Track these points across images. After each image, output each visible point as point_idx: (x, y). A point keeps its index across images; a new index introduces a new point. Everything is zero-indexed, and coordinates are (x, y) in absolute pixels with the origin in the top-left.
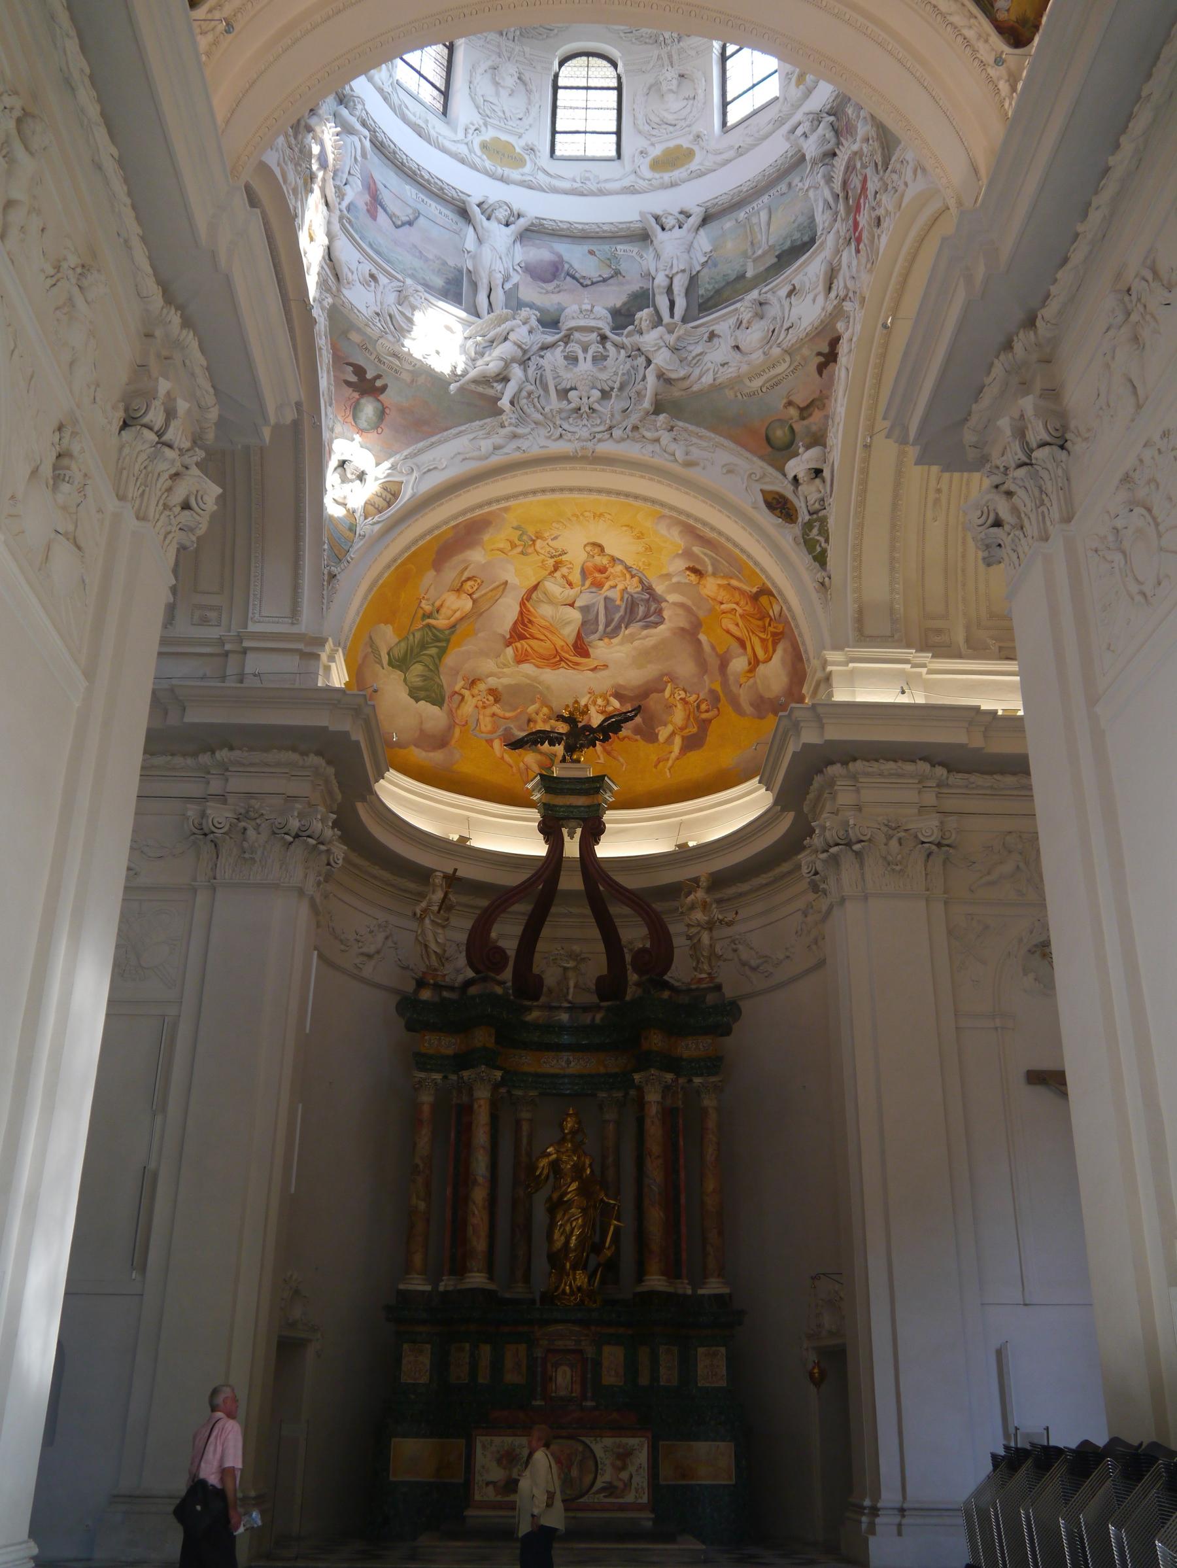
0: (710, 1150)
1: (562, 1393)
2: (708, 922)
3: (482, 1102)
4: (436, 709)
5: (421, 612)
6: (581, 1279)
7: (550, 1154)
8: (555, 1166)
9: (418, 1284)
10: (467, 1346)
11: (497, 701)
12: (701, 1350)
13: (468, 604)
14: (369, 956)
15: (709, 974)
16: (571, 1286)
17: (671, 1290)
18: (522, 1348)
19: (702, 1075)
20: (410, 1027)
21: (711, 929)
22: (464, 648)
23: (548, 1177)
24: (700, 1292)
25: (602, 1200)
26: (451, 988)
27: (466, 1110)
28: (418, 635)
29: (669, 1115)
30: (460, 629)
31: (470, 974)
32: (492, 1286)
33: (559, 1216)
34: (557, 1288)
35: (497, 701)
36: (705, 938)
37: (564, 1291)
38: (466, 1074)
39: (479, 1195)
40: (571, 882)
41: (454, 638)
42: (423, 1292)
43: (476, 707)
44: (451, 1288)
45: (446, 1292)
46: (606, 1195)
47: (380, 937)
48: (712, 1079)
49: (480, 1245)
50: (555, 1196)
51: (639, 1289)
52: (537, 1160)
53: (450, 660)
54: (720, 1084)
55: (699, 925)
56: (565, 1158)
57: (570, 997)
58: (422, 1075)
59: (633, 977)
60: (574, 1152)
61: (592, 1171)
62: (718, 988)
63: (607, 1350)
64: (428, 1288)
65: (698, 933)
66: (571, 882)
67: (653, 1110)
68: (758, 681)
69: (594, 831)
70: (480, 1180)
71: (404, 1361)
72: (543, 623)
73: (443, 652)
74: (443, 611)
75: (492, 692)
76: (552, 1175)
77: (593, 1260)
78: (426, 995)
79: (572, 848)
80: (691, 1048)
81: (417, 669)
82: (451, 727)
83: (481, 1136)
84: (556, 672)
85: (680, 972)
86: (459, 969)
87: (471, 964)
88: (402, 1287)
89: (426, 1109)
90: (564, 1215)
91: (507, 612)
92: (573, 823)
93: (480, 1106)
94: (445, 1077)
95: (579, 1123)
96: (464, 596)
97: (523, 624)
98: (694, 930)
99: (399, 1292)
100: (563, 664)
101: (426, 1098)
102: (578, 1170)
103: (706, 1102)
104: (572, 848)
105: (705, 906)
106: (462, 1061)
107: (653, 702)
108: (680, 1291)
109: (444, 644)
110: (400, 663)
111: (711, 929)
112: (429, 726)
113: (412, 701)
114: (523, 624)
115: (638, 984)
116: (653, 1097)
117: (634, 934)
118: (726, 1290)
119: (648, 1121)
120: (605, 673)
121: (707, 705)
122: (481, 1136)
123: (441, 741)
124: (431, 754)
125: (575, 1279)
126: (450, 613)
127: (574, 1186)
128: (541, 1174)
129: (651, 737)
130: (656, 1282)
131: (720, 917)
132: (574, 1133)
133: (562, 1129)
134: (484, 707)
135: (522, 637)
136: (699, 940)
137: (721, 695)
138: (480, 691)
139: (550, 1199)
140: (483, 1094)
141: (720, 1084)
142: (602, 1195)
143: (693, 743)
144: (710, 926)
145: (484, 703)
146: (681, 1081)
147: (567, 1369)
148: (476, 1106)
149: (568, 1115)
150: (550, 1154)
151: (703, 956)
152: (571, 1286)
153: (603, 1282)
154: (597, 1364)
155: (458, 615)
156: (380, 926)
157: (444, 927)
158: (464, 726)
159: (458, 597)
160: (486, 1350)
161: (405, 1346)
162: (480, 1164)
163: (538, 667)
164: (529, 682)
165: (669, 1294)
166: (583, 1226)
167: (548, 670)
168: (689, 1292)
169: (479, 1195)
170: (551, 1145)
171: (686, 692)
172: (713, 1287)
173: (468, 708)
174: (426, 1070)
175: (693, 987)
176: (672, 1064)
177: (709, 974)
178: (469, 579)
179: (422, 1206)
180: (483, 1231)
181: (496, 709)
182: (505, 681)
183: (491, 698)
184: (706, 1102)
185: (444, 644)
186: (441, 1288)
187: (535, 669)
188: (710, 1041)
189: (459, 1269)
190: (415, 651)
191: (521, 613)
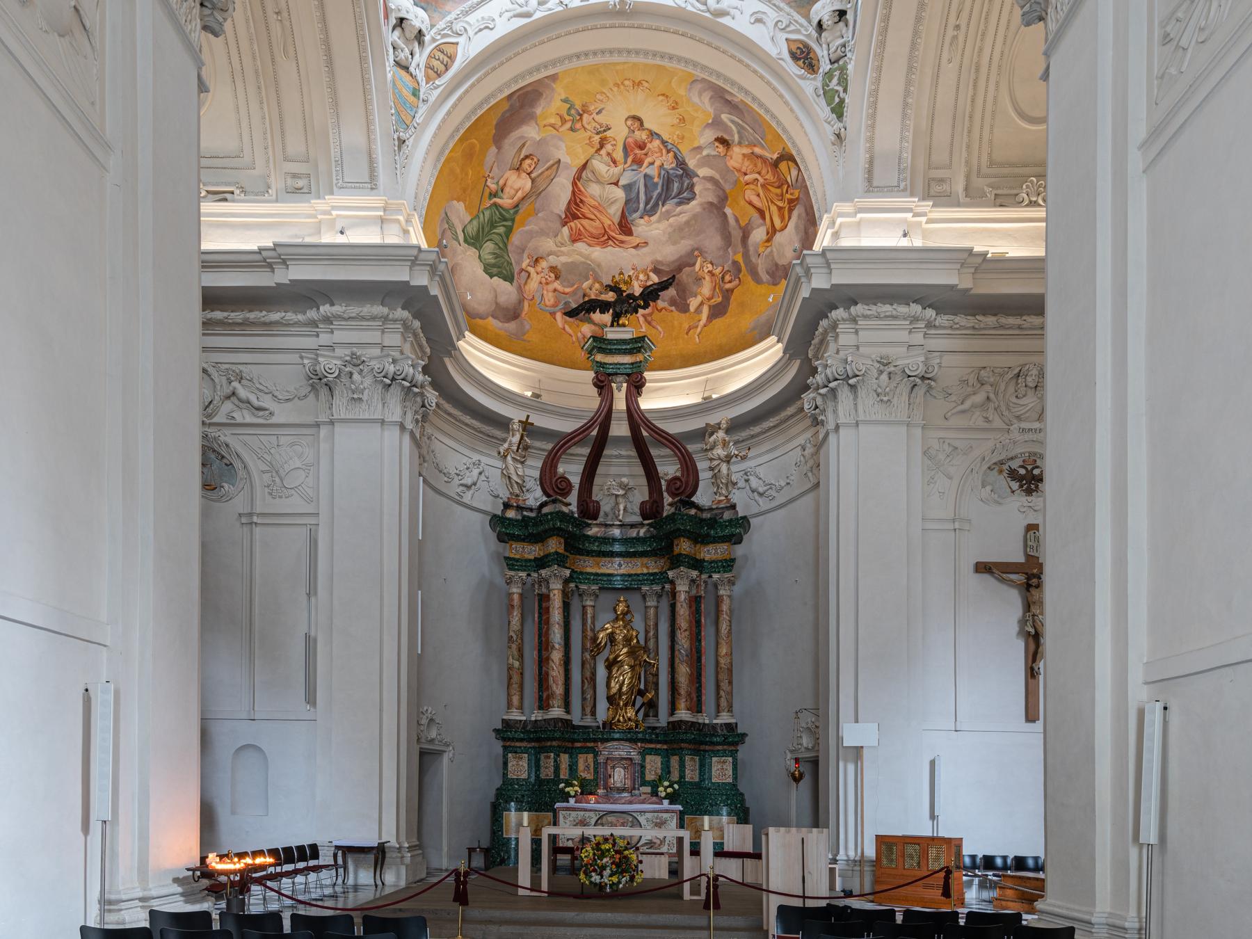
0: (724, 626)
1: (618, 785)
2: (726, 456)
3: (556, 592)
6: (630, 713)
7: (607, 629)
8: (611, 638)
9: (515, 715)
10: (552, 754)
11: (557, 278)
12: (714, 759)
14: (468, 487)
15: (726, 497)
16: (623, 716)
17: (694, 720)
18: (590, 756)
19: (719, 572)
20: (502, 538)
21: (728, 462)
23: (606, 644)
24: (715, 721)
25: (645, 661)
26: (531, 510)
27: (544, 599)
29: (695, 602)
31: (545, 499)
32: (568, 717)
33: (614, 671)
34: (613, 719)
35: (557, 278)
36: (724, 467)
37: (619, 721)
38: (543, 572)
39: (556, 656)
40: (619, 428)
42: (521, 721)
43: (541, 283)
44: (540, 718)
45: (536, 721)
46: (648, 657)
47: (476, 472)
48: (727, 575)
49: (558, 690)
50: (611, 657)
51: (671, 719)
52: (598, 632)
54: (732, 579)
55: (720, 459)
56: (618, 631)
57: (621, 517)
58: (512, 573)
59: (668, 499)
60: (625, 627)
61: (638, 641)
62: (733, 507)
63: (648, 758)
64: (524, 718)
65: (719, 465)
66: (619, 428)
67: (682, 597)
68: (774, 250)
69: (637, 386)
70: (557, 646)
71: (510, 765)
75: (553, 269)
76: (609, 644)
77: (639, 701)
78: (511, 514)
79: (620, 404)
80: (710, 553)
82: (521, 301)
83: (556, 616)
84: (606, 250)
85: (704, 497)
86: (534, 497)
87: (545, 493)
88: (505, 717)
89: (516, 597)
90: (618, 670)
92: (620, 378)
93: (554, 595)
94: (529, 575)
95: (628, 607)
98: (716, 463)
99: (503, 720)
100: (610, 242)
101: (516, 590)
102: (627, 640)
103: (721, 592)
104: (620, 404)
105: (725, 444)
106: (541, 563)
107: (684, 276)
108: (700, 721)
111: (728, 462)
115: (671, 505)
116: (682, 588)
117: (668, 468)
118: (733, 721)
119: (678, 605)
120: (645, 250)
121: (731, 276)
122: (556, 616)
123: (512, 314)
125: (626, 713)
127: (625, 650)
128: (600, 643)
129: (684, 308)
130: (683, 714)
131: (736, 452)
132: (625, 614)
133: (615, 611)
134: (547, 284)
136: (719, 471)
137: (743, 265)
138: (543, 269)
139: (607, 659)
140: (556, 587)
141: (732, 579)
142: (645, 657)
143: (718, 311)
144: (728, 459)
145: (546, 279)
146: (704, 576)
147: (622, 770)
148: (552, 595)
149: (620, 601)
150: (607, 629)
151: (722, 483)
152: (623, 716)
153: (646, 715)
154: (643, 767)
156: (474, 463)
157: (522, 463)
158: (532, 300)
160: (565, 759)
161: (510, 755)
162: (557, 635)
163: (590, 245)
164: (583, 260)
165: (693, 722)
166: (631, 678)
167: (598, 248)
168: (707, 722)
169: (556, 656)
170: (608, 623)
171: (712, 264)
172: (724, 718)
173: (533, 285)
174: (515, 570)
175: (714, 507)
176: (697, 564)
177: (726, 497)
179: (517, 664)
180: (561, 680)
181: (557, 285)
182: (563, 259)
183: (552, 275)
184: (721, 592)
186: (533, 719)
187: (587, 247)
188: (726, 547)
189: (543, 704)
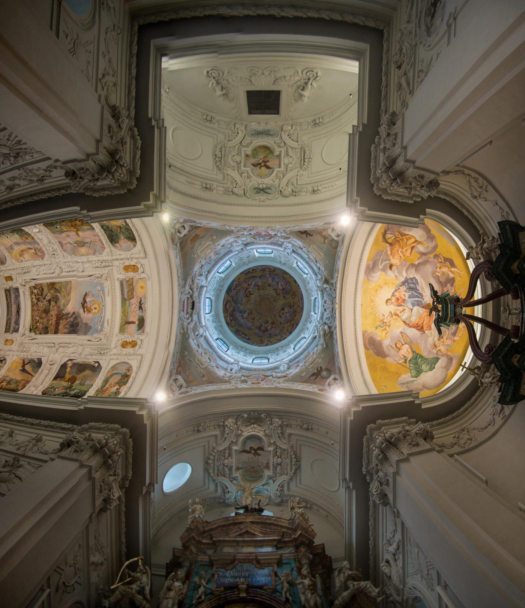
4: (440, 361)
5: (403, 364)
13: (407, 346)
22: (422, 349)
28: (411, 365)
30: (415, 349)
41: (418, 352)
53: (425, 354)
72: (418, 320)
73: (421, 357)
74: (405, 355)
81: (424, 367)
91: (413, 333)
96: (402, 347)
97: (417, 327)
109: (418, 356)
110: (419, 372)
112: (444, 364)
113: (434, 370)
114: (417, 327)
124: (453, 364)
126: (407, 353)
135: (422, 327)
155: (409, 350)
159: (402, 349)
178: (396, 345)
185: (418, 356)
190: (417, 367)
191: (414, 327)
